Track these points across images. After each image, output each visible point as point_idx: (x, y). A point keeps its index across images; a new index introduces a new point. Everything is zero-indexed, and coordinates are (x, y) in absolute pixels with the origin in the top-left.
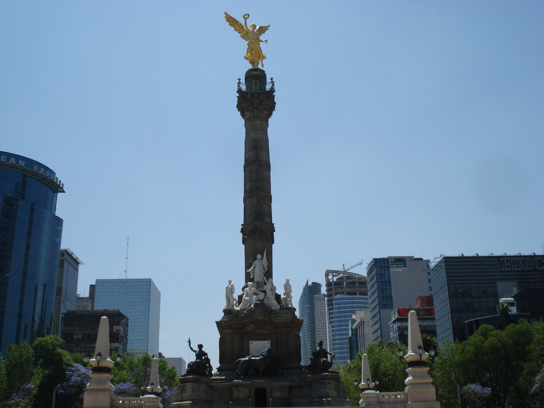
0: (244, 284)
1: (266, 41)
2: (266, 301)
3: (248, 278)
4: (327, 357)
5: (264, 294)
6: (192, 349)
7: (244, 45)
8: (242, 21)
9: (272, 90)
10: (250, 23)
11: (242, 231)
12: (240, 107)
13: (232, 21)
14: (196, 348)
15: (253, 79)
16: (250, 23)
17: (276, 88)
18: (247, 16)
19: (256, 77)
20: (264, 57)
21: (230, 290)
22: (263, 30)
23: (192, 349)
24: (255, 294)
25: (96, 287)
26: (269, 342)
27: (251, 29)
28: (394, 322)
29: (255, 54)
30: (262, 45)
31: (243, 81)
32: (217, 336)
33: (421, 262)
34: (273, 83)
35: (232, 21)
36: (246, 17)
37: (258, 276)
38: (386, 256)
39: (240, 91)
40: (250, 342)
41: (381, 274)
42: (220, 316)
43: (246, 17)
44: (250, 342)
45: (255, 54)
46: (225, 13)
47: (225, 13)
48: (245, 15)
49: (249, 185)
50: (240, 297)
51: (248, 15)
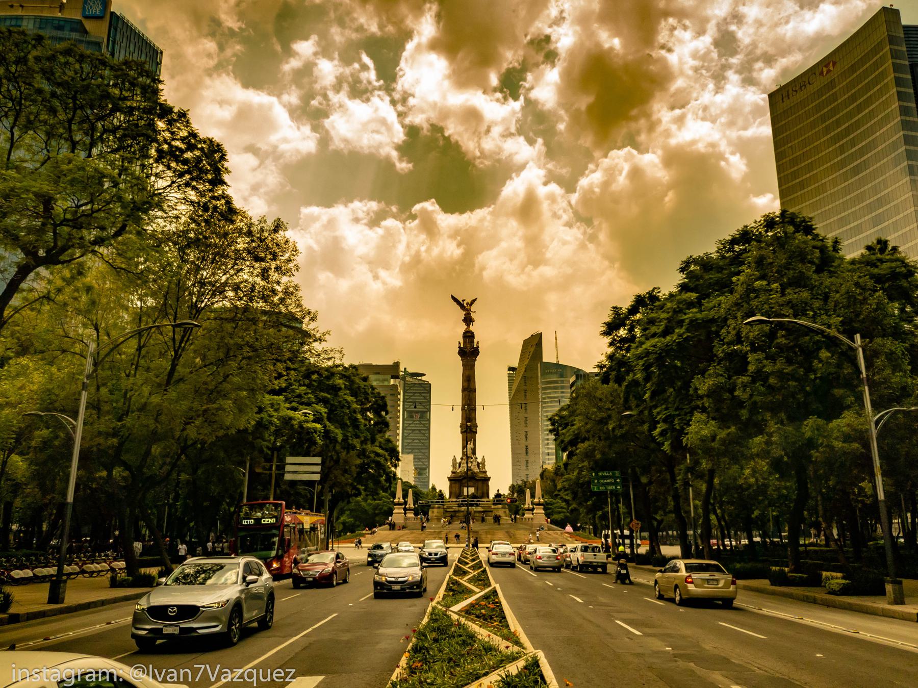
0: (461, 456)
3: (465, 454)
7: (462, 314)
9: (478, 347)
12: (459, 353)
19: (469, 336)
21: (454, 460)
29: (468, 320)
30: (473, 315)
31: (462, 341)
32: (448, 483)
37: (469, 453)
39: (460, 347)
42: (450, 474)
45: (468, 320)
50: (460, 464)
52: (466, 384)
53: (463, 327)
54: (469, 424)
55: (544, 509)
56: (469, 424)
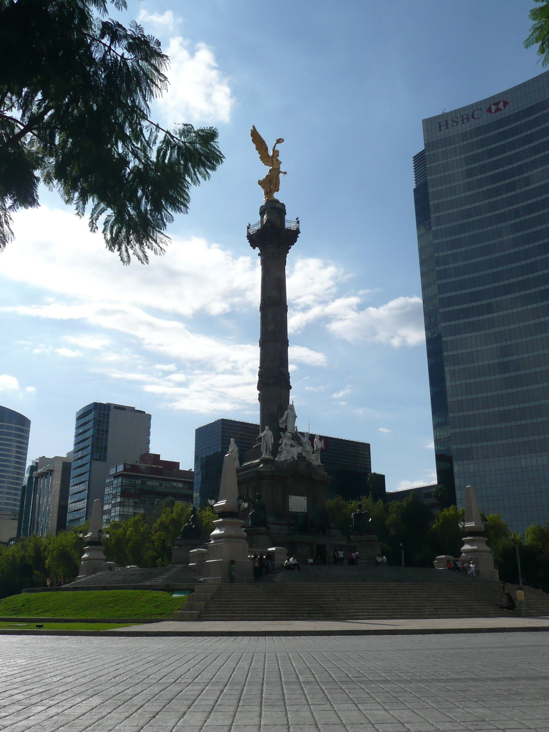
1: (285, 173)
2: (304, 454)
9: (297, 232)
13: (256, 136)
15: (277, 212)
16: (278, 147)
20: (277, 191)
24: (292, 446)
26: (306, 498)
28: (116, 476)
30: (281, 175)
33: (143, 415)
34: (298, 222)
35: (256, 136)
36: (279, 141)
38: (105, 402)
40: (290, 496)
41: (99, 422)
43: (279, 141)
44: (290, 496)
46: (254, 127)
47: (254, 127)
48: (280, 139)
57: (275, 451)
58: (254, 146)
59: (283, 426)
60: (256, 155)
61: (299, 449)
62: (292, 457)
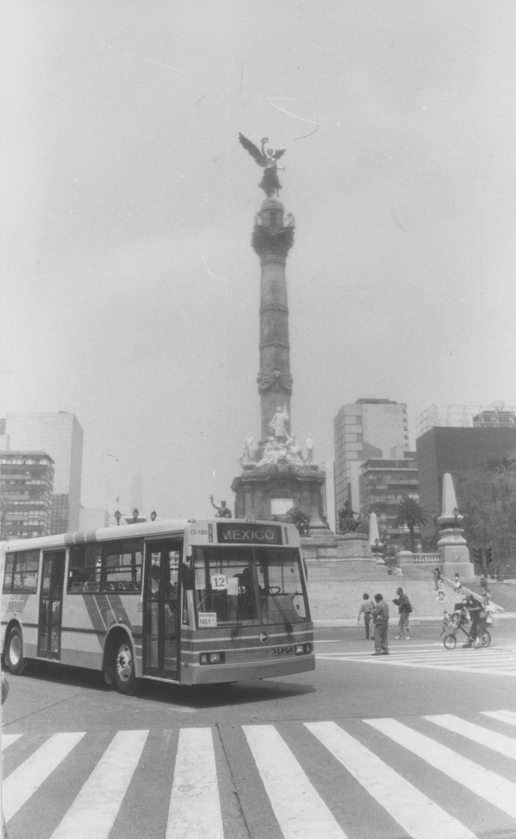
0: (259, 439)
1: (284, 169)
2: (289, 457)
4: (352, 517)
5: (286, 449)
6: (214, 506)
8: (259, 145)
9: (293, 228)
10: (267, 147)
11: (259, 380)
14: (219, 505)
16: (267, 147)
17: (297, 224)
18: (266, 140)
22: (279, 154)
23: (214, 506)
24: (277, 449)
25: (8, 422)
27: (266, 154)
29: (271, 183)
36: (264, 141)
42: (239, 472)
43: (264, 141)
46: (240, 134)
47: (240, 134)
48: (264, 139)
49: (266, 332)
51: (267, 139)
52: (269, 297)
53: (261, 196)
54: (277, 373)
55: (463, 535)
56: (277, 373)
57: (259, 455)
58: (247, 152)
59: (272, 431)
60: (250, 160)
61: (283, 453)
62: (273, 461)
